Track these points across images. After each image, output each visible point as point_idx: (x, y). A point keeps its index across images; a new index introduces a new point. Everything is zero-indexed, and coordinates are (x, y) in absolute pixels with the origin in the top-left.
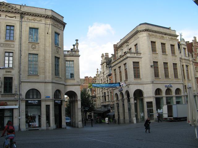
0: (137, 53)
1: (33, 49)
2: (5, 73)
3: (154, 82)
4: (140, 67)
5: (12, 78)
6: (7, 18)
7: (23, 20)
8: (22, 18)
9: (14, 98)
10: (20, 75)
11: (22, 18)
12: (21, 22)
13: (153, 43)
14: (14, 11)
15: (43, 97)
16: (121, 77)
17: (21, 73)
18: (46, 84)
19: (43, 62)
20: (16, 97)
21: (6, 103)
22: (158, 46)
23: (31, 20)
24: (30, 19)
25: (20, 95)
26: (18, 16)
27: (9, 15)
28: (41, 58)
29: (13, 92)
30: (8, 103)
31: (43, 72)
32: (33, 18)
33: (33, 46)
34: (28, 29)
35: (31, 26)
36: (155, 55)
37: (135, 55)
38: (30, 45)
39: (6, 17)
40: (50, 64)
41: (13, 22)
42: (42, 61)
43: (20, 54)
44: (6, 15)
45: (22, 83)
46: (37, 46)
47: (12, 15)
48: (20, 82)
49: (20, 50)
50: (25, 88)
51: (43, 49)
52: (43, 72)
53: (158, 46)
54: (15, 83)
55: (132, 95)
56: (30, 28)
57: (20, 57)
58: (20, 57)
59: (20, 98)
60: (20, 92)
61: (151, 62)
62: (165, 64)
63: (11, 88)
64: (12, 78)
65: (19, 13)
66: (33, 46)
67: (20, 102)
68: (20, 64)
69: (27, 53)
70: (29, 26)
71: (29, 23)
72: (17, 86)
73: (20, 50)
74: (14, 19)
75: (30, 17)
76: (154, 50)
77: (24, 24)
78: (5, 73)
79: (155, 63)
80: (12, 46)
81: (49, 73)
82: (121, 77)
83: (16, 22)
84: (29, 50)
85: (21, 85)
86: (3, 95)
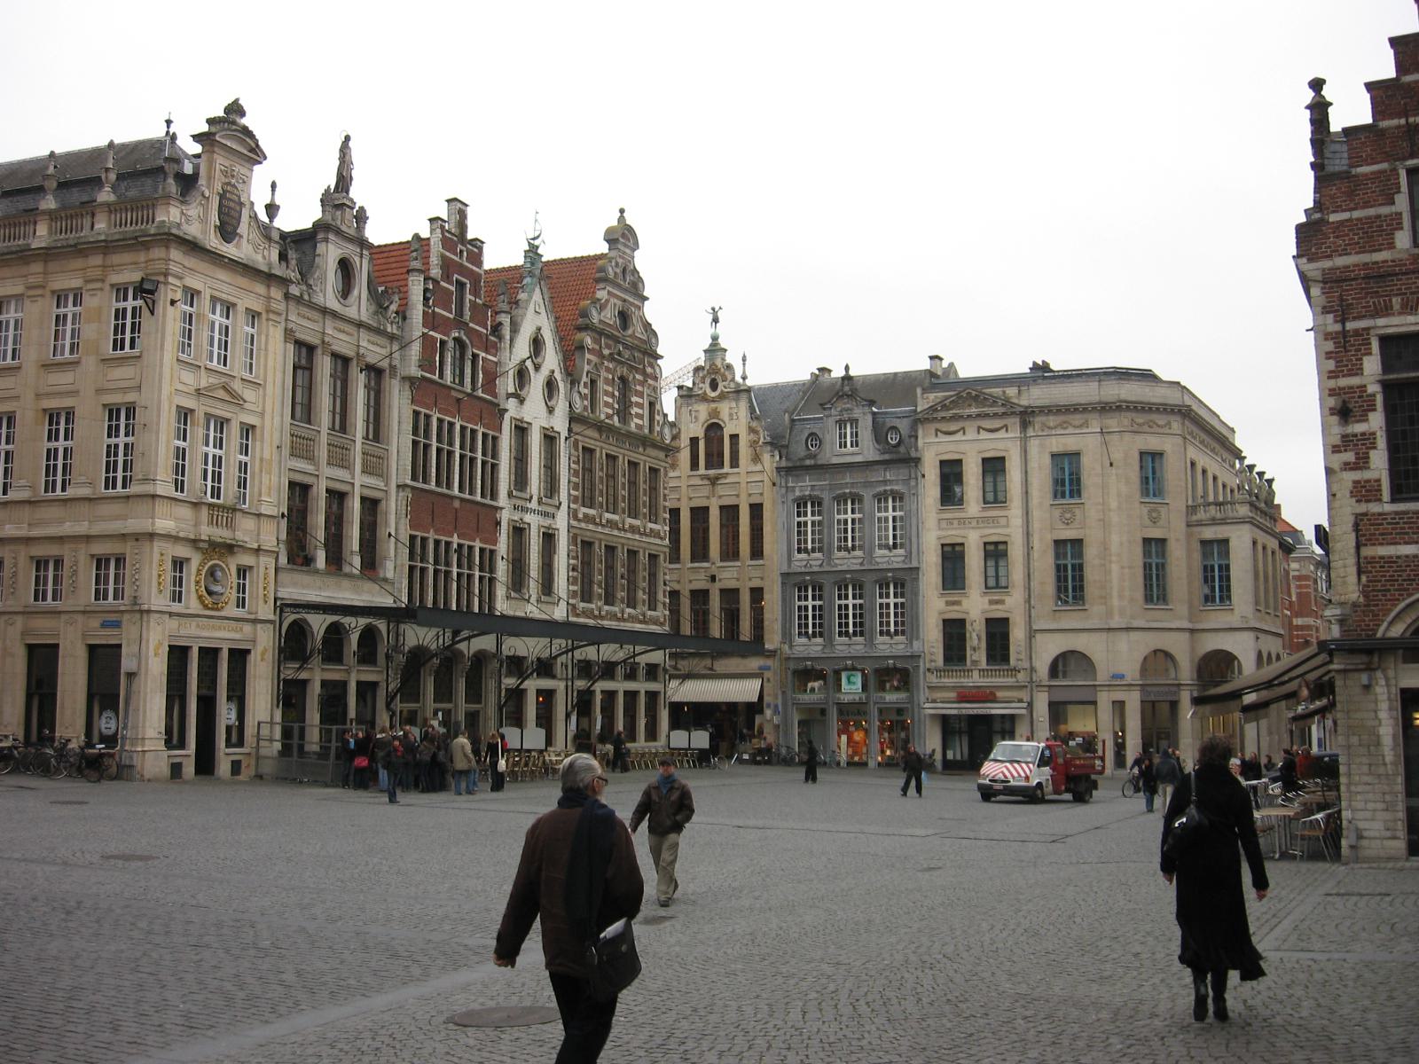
2: (987, 606)
5: (1007, 620)
6: (984, 435)
7: (1030, 432)
8: (1025, 425)
9: (1014, 680)
10: (1030, 610)
11: (1025, 425)
12: (1024, 441)
15: (1102, 677)
17: (1032, 602)
18: (1111, 634)
20: (1021, 676)
21: (993, 694)
23: (1055, 427)
24: (1052, 424)
25: (1033, 670)
26: (1014, 422)
27: (988, 424)
28: (1091, 554)
29: (1012, 662)
30: (1000, 694)
31: (1101, 597)
32: (1060, 418)
33: (1068, 516)
34: (1047, 460)
35: (1055, 450)
38: (1057, 513)
39: (979, 433)
41: (1000, 445)
42: (1097, 562)
43: (1028, 544)
44: (979, 428)
45: (1038, 636)
46: (1077, 511)
47: (997, 423)
48: (1032, 634)
49: (1028, 534)
50: (1049, 649)
51: (1100, 520)
52: (1101, 597)
54: (1017, 634)
56: (1052, 456)
57: (1028, 554)
58: (1028, 554)
59: (1031, 679)
60: (1031, 663)
63: (1006, 647)
64: (1007, 620)
65: (1013, 413)
66: (1068, 516)
67: (1032, 689)
68: (1029, 575)
69: (1049, 538)
70: (1049, 450)
71: (1048, 441)
72: (1023, 643)
73: (1028, 534)
74: (1001, 434)
75: (1052, 420)
77: (1034, 445)
78: (987, 606)
80: (1003, 521)
83: (1009, 444)
84: (1053, 529)
85: (1033, 640)
86: (983, 670)
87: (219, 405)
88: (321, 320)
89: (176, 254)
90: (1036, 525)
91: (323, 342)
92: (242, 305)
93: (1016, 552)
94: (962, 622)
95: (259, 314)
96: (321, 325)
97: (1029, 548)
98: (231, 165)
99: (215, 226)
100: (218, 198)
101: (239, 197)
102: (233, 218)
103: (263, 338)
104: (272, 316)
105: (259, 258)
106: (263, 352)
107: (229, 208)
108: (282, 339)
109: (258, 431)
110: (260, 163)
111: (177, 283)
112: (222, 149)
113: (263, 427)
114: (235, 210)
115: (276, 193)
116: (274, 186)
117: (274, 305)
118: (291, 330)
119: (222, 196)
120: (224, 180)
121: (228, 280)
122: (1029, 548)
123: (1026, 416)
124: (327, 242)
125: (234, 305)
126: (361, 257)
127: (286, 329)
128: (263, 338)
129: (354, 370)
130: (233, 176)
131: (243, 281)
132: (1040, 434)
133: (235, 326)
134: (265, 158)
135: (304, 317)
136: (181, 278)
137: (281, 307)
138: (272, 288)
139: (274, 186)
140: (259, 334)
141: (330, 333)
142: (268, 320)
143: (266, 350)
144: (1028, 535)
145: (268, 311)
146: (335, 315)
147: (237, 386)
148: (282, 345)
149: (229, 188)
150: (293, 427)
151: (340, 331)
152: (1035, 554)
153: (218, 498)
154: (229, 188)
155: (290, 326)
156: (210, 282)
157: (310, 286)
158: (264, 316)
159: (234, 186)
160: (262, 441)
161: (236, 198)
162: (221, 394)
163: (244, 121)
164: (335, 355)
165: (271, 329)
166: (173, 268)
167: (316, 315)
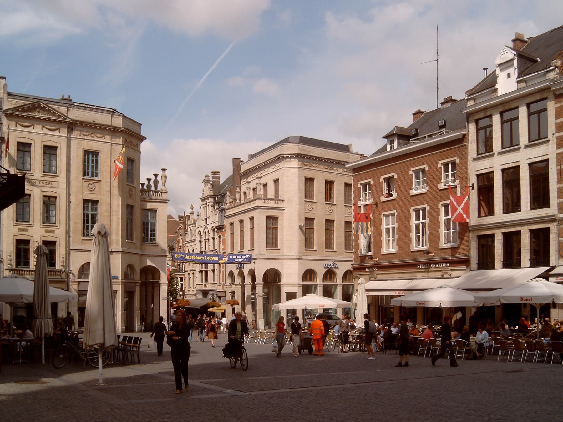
0: (277, 199)
1: (91, 191)
3: (303, 257)
4: (279, 227)
13: (309, 181)
14: (58, 119)
16: (242, 246)
19: (108, 216)
22: (319, 188)
33: (91, 186)
36: (308, 206)
37: (273, 204)
40: (119, 219)
51: (108, 191)
53: (319, 188)
55: (259, 279)
61: (300, 220)
62: (329, 223)
66: (91, 186)
76: (308, 194)
79: (309, 221)
80: (55, 184)
81: (117, 234)
82: (242, 246)
84: (83, 193)
90: (73, 189)
93: (61, 203)
94: (27, 242)
97: (69, 202)
122: (69, 202)
123: (72, 126)
132: (78, 137)
144: (68, 194)
152: (72, 206)
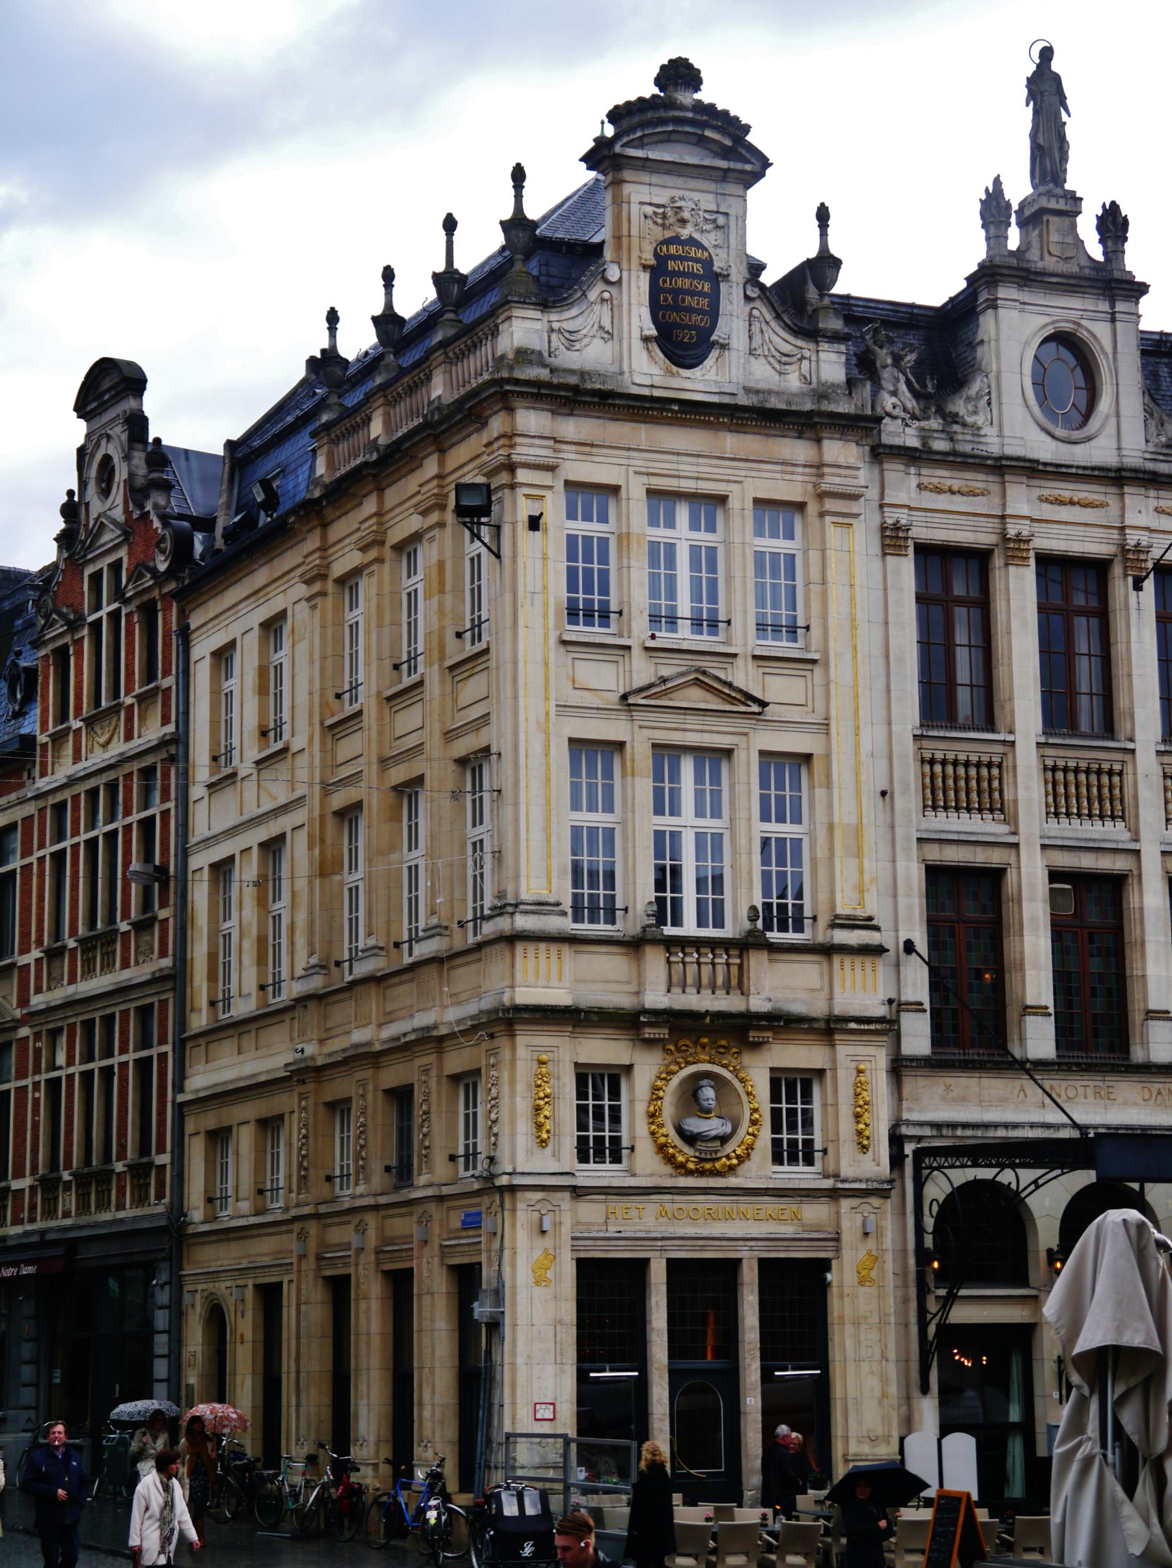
87: (692, 721)
88: (995, 488)
89: (531, 420)
91: (1004, 538)
92: (740, 500)
95: (801, 507)
96: (997, 500)
98: (673, 200)
99: (646, 339)
100: (645, 278)
101: (708, 263)
102: (690, 310)
103: (814, 556)
104: (831, 505)
105: (793, 382)
106: (815, 589)
107: (676, 292)
108: (876, 548)
109: (817, 764)
110: (758, 176)
111: (544, 478)
112: (643, 168)
113: (828, 757)
114: (702, 294)
115: (830, 231)
116: (823, 215)
117: (832, 481)
118: (897, 527)
119: (658, 271)
120: (659, 234)
121: (695, 448)
124: (995, 307)
125: (722, 500)
126: (1113, 320)
127: (883, 529)
128: (814, 556)
129: (1120, 587)
130: (683, 222)
131: (731, 442)
133: (727, 542)
134: (765, 163)
135: (938, 490)
136: (551, 468)
137: (864, 476)
138: (826, 443)
139: (823, 215)
140: (805, 552)
141: (1025, 511)
142: (822, 515)
143: (824, 582)
145: (822, 496)
146: (1032, 469)
147: (743, 676)
148: (877, 564)
149: (673, 250)
150: (925, 743)
151: (1060, 502)
153: (719, 923)
154: (673, 250)
155: (891, 516)
156: (639, 461)
157: (954, 418)
158: (812, 509)
159: (692, 242)
160: (829, 785)
161: (697, 268)
162: (695, 697)
163: (706, 95)
164: (1048, 563)
165: (834, 535)
166: (525, 451)
167: (978, 480)
